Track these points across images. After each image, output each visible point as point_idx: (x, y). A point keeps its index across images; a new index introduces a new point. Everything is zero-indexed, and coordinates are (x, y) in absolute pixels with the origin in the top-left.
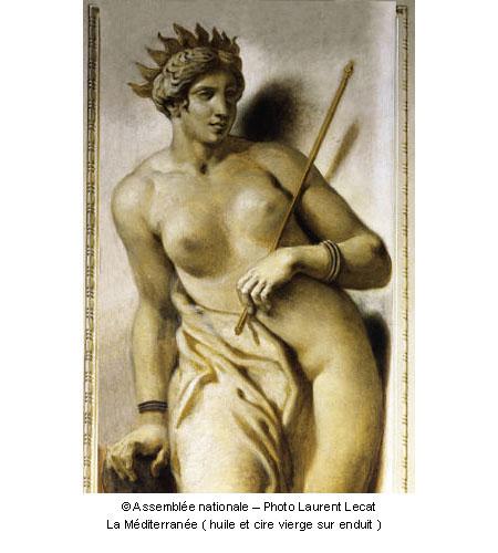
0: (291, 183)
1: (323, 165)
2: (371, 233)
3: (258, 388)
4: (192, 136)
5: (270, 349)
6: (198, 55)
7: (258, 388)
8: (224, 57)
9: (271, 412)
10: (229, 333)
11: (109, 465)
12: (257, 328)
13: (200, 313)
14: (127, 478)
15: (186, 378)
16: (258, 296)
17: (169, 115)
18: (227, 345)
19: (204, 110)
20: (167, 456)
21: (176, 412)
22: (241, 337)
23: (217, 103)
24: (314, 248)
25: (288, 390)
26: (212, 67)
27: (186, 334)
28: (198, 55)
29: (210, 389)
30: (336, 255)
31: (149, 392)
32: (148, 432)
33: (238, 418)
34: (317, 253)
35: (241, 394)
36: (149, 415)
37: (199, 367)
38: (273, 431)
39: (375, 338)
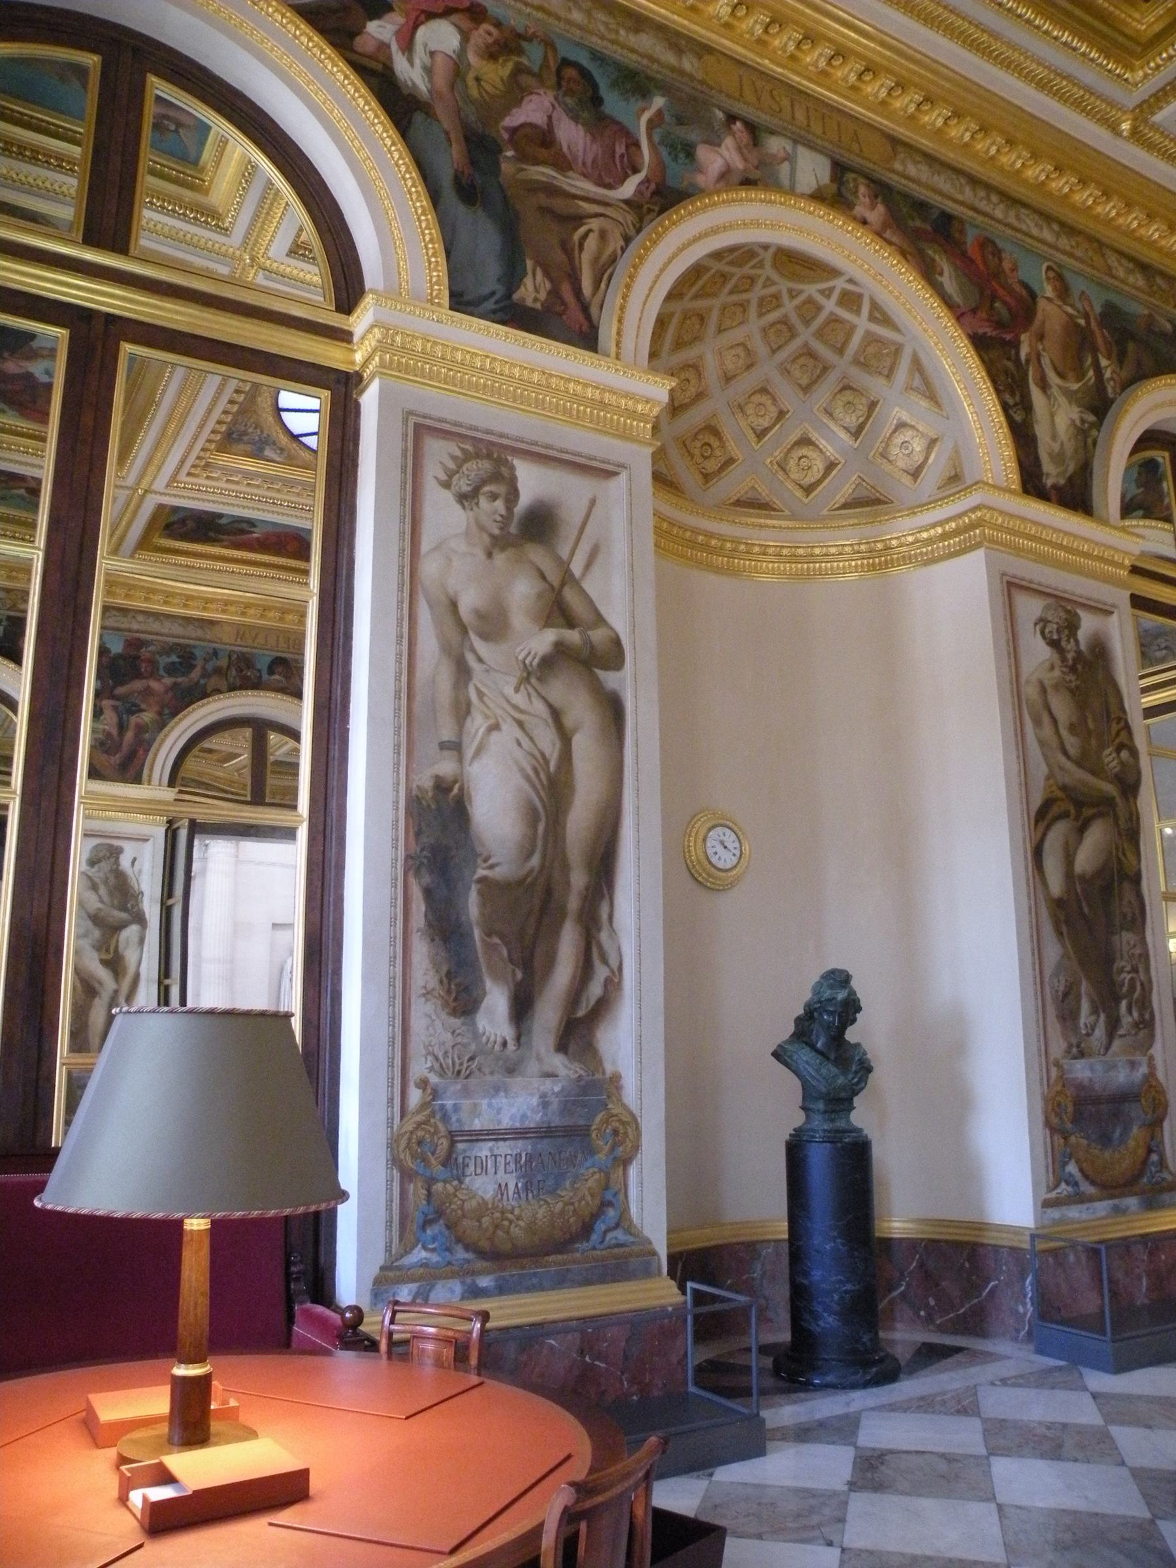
0: (554, 578)
1: (576, 568)
2: (612, 629)
3: (531, 739)
4: (482, 528)
5: (539, 707)
6: (486, 465)
7: (531, 739)
8: (504, 470)
9: (541, 761)
10: (509, 691)
11: (414, 793)
12: (529, 687)
13: (487, 671)
14: (429, 806)
15: (477, 724)
16: (531, 664)
17: (464, 508)
18: (508, 701)
19: (490, 508)
20: (461, 789)
21: (469, 752)
22: (519, 696)
23: (499, 505)
24: (570, 631)
25: (554, 745)
26: (496, 477)
27: (477, 689)
28: (486, 465)
29: (495, 735)
30: (588, 642)
31: (447, 734)
32: (446, 767)
33: (517, 762)
34: (573, 636)
35: (519, 744)
36: (446, 753)
37: (487, 717)
38: (543, 776)
39: (613, 710)
